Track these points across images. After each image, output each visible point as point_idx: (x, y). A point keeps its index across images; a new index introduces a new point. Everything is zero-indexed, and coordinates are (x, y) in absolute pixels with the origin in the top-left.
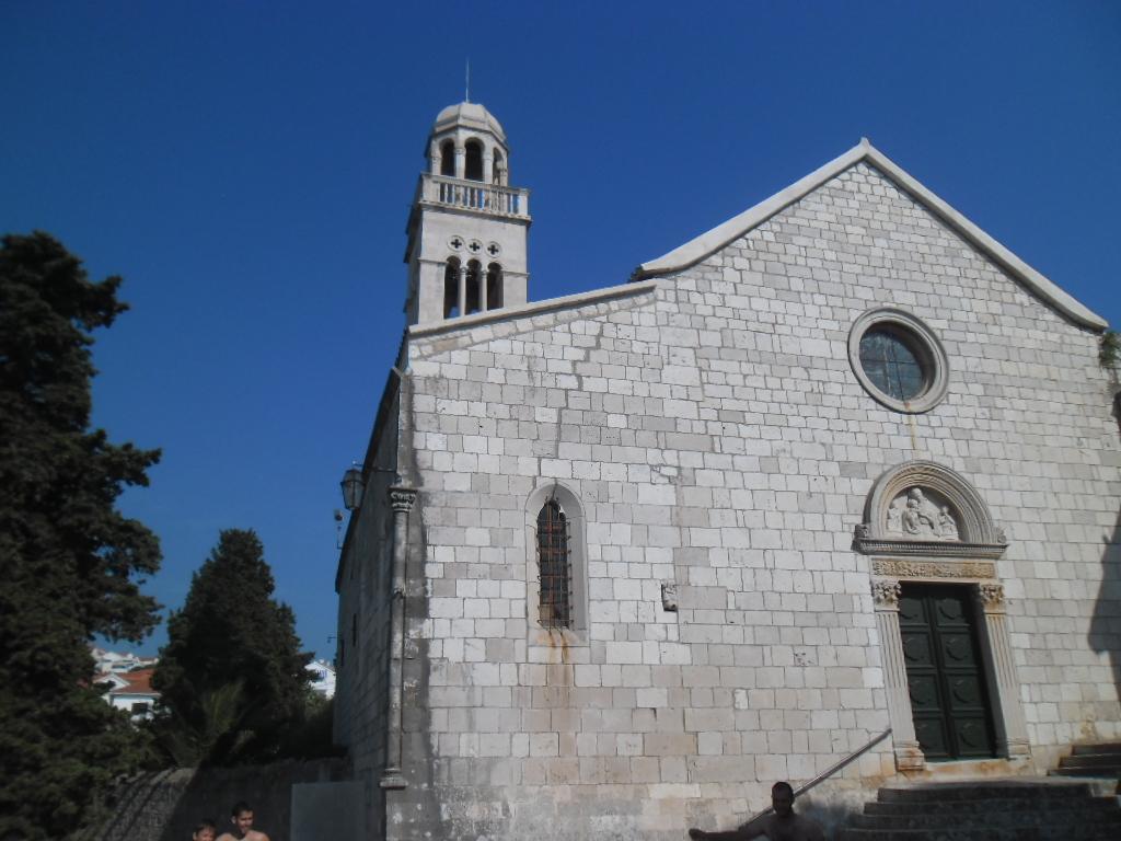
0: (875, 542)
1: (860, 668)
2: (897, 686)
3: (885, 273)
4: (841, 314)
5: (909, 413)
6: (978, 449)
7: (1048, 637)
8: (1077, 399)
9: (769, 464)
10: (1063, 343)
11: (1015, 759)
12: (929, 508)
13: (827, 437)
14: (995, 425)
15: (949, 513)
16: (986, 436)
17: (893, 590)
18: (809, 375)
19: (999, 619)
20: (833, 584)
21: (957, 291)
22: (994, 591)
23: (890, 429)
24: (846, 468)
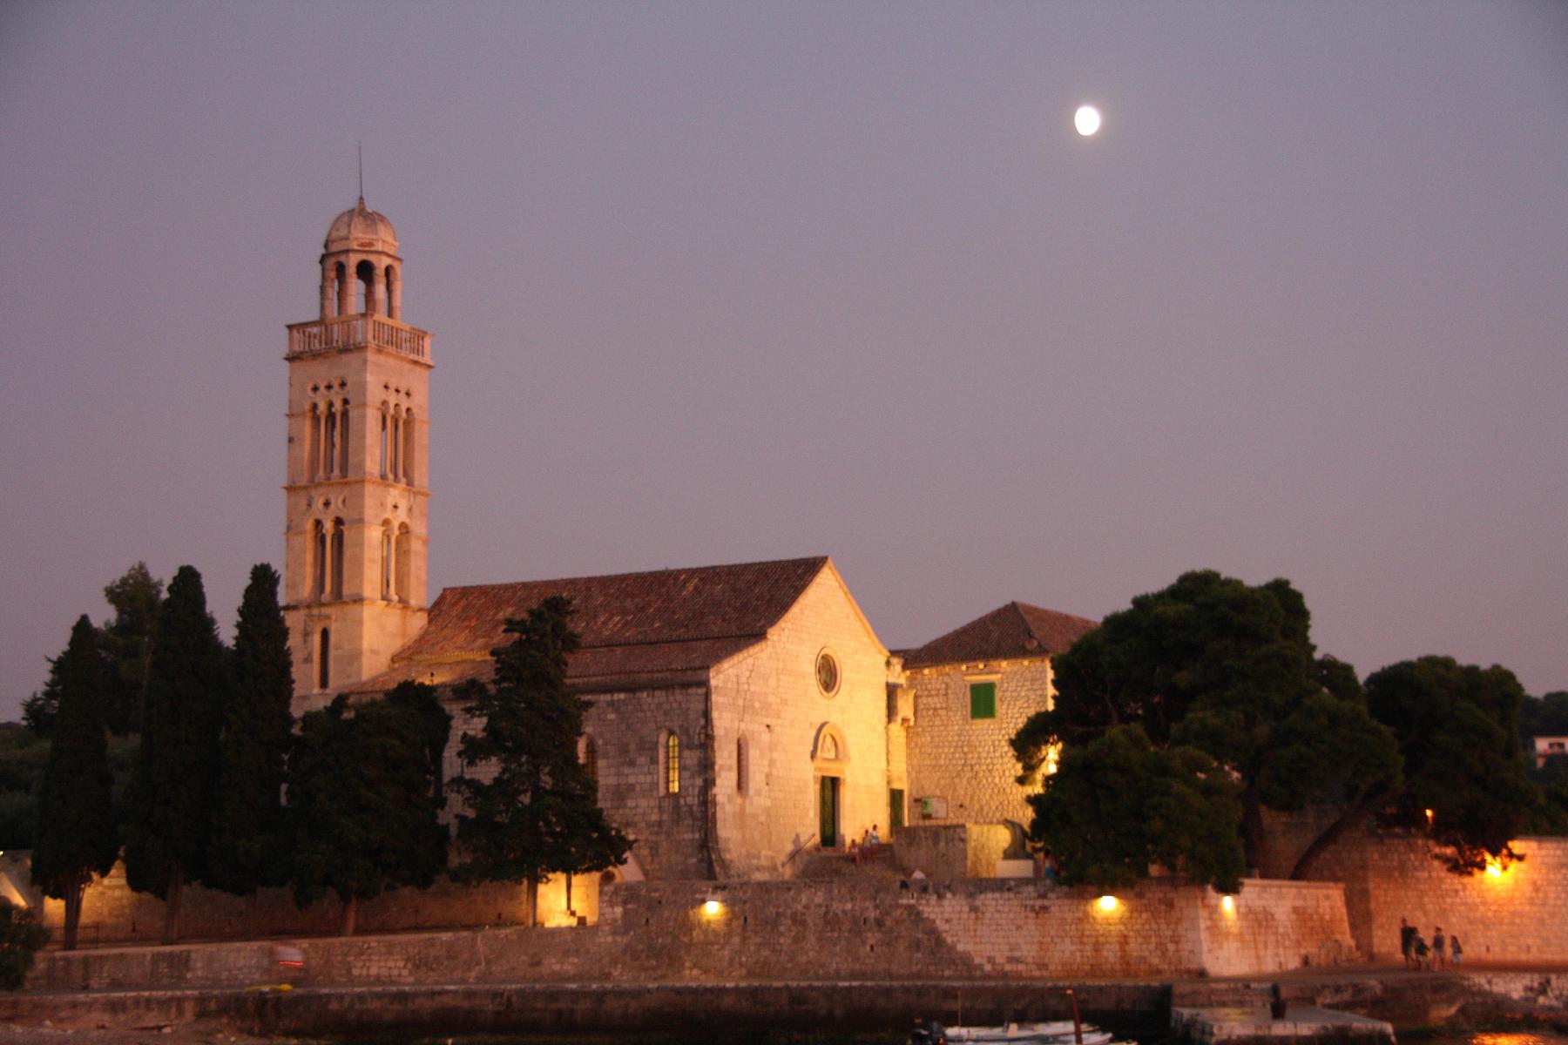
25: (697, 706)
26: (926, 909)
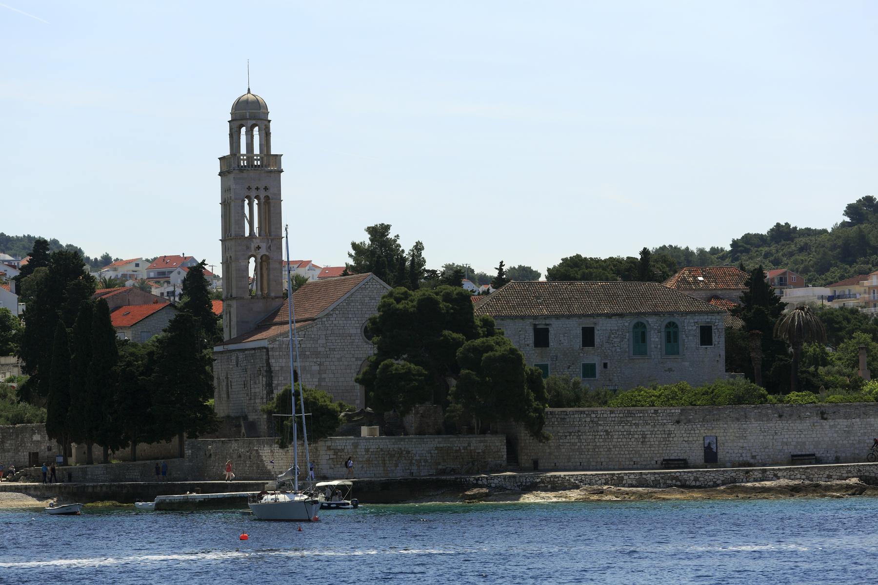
3: (373, 309)
9: (340, 360)
13: (353, 352)
24: (357, 359)
25: (264, 357)
26: (261, 451)
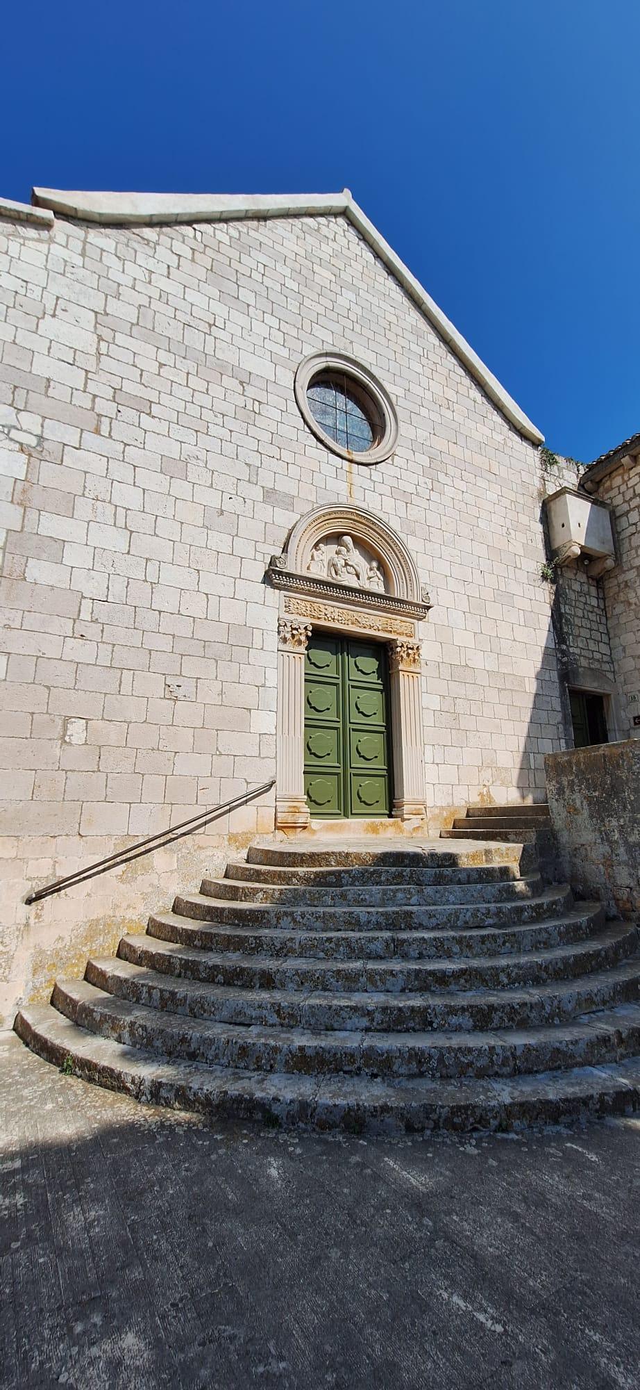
0: (289, 575)
1: (250, 710)
2: (292, 732)
4: (296, 345)
5: (351, 461)
6: (414, 513)
7: (458, 700)
8: (512, 496)
10: (505, 444)
11: (409, 819)
12: (356, 557)
13: (255, 460)
14: (434, 496)
15: (378, 569)
16: (425, 504)
17: (302, 631)
18: (244, 390)
19: (411, 678)
20: (233, 612)
21: (419, 368)
22: (412, 649)
23: (328, 470)
